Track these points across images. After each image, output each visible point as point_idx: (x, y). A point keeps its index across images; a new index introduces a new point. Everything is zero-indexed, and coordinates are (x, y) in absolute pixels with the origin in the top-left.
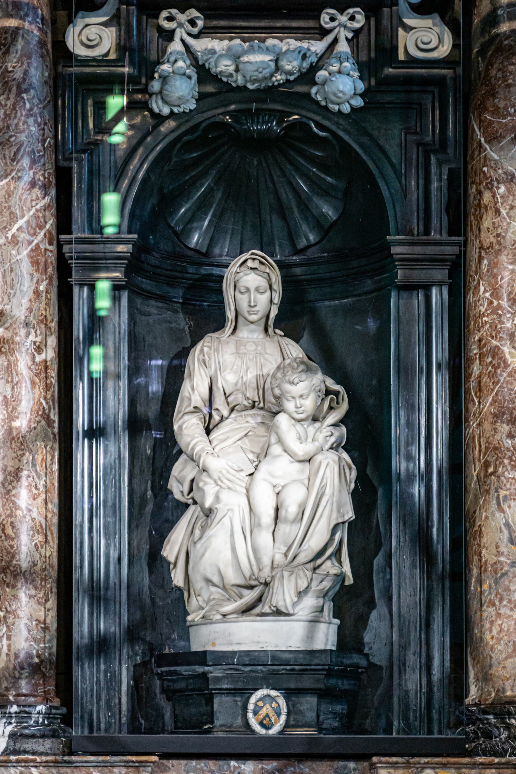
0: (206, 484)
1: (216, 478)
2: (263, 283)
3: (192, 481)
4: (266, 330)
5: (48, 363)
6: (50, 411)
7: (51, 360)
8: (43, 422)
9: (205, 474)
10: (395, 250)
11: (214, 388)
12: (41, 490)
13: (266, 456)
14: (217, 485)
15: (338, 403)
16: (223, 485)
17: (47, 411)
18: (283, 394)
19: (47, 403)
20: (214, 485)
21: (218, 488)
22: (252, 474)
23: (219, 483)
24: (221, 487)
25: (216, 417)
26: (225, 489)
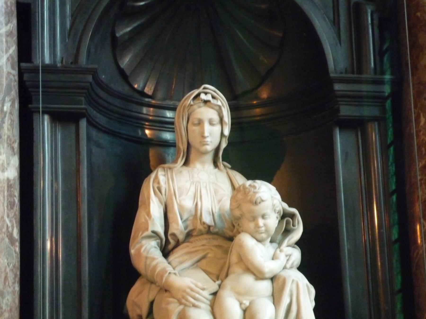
0: (168, 303)
1: (180, 296)
2: (215, 117)
3: (152, 304)
4: (216, 165)
5: (12, 182)
6: (13, 230)
7: (14, 179)
8: (7, 240)
9: (167, 294)
10: (337, 87)
11: (170, 215)
12: (4, 308)
13: (227, 276)
14: (181, 303)
15: (294, 225)
16: (187, 303)
17: (10, 229)
18: (242, 215)
19: (11, 221)
20: (178, 304)
21: (182, 307)
22: (215, 294)
23: (183, 301)
24: (186, 305)
25: (172, 242)
26: (190, 307)
